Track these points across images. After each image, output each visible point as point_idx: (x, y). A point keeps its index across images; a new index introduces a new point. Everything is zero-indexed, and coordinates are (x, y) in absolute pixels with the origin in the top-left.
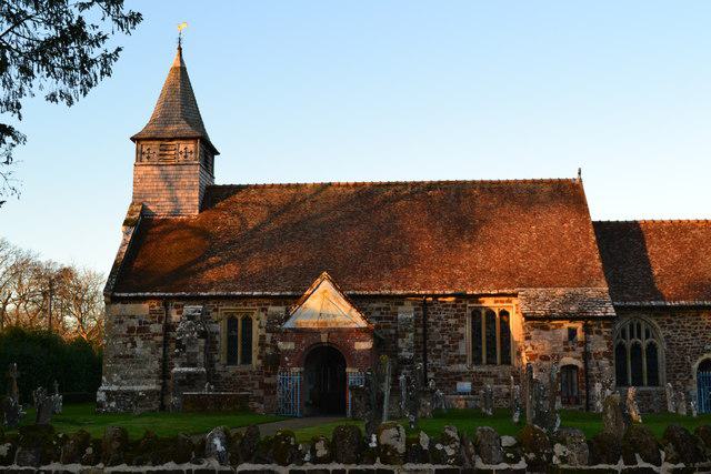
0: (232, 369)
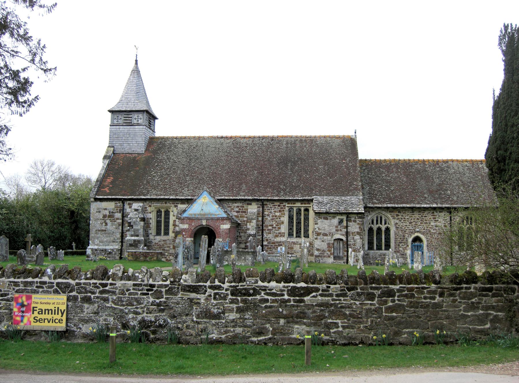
0: (158, 238)
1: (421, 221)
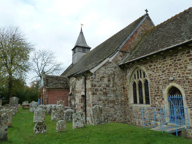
1: (174, 66)
